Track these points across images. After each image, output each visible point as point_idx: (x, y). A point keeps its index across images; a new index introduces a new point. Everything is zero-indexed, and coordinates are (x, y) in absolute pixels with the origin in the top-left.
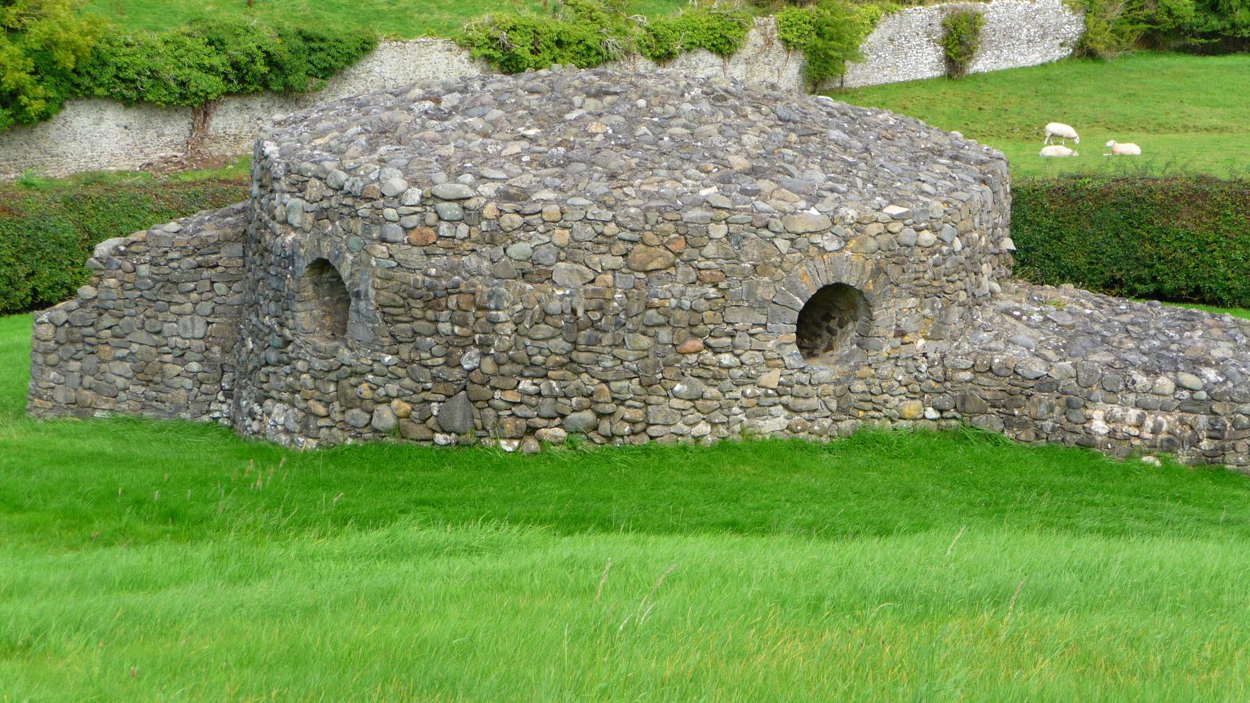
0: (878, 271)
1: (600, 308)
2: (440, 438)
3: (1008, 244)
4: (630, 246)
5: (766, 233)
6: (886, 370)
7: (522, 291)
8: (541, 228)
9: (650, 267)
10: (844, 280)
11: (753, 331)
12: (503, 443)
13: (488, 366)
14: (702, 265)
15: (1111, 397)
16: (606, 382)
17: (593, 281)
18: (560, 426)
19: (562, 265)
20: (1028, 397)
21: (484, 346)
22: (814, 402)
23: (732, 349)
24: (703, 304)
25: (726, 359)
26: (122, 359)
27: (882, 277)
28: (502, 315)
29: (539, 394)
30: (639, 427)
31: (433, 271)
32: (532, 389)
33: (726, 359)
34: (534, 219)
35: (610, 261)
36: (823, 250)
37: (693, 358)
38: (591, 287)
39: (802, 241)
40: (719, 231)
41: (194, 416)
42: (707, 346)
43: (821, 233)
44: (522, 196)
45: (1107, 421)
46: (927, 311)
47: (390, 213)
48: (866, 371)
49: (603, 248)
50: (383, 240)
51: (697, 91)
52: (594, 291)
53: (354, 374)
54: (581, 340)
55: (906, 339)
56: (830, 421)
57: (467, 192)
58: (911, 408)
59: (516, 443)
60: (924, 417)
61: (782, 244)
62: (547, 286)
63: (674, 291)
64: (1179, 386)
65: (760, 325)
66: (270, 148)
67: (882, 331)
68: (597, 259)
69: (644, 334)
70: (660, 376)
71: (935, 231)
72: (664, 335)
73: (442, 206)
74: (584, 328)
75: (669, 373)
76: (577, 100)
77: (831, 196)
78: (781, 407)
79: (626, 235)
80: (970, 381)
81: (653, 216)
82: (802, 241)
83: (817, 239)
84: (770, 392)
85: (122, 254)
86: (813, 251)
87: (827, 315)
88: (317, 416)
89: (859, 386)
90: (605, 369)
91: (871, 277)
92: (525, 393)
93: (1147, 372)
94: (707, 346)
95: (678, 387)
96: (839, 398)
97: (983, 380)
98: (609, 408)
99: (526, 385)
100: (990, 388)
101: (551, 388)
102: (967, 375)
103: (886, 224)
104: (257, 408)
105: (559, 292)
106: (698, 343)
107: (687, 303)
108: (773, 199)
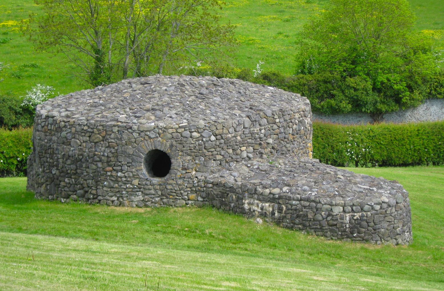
0: (172, 146)
4: (90, 134)
5: (130, 130)
6: (180, 182)
7: (63, 148)
8: (68, 127)
9: (95, 141)
11: (128, 165)
12: (62, 199)
13: (57, 173)
14: (109, 141)
15: (251, 196)
16: (86, 180)
17: (81, 146)
18: (75, 194)
19: (73, 139)
20: (228, 194)
21: (57, 166)
22: (153, 192)
23: (121, 171)
24: (110, 155)
25: (119, 174)
28: (60, 156)
29: (69, 183)
30: (95, 196)
32: (68, 181)
33: (119, 174)
36: (150, 138)
37: (109, 174)
38: (80, 147)
40: (116, 129)
43: (149, 131)
45: (249, 204)
46: (197, 161)
48: (171, 181)
49: (83, 134)
52: (81, 149)
54: (78, 165)
55: (188, 171)
56: (159, 198)
59: (65, 199)
60: (198, 200)
61: (135, 135)
62: (69, 147)
65: (130, 163)
67: (175, 167)
68: (81, 138)
69: (94, 164)
70: (99, 179)
71: (199, 132)
72: (100, 165)
78: (140, 193)
79: (89, 130)
80: (211, 188)
82: (142, 134)
83: (148, 133)
84: (135, 186)
86: (147, 138)
90: (85, 176)
91: (170, 148)
92: (66, 183)
96: (162, 190)
97: (215, 187)
98: (87, 189)
101: (73, 182)
102: (210, 185)
103: (176, 129)
105: (72, 149)
106: (111, 168)
107: (106, 154)
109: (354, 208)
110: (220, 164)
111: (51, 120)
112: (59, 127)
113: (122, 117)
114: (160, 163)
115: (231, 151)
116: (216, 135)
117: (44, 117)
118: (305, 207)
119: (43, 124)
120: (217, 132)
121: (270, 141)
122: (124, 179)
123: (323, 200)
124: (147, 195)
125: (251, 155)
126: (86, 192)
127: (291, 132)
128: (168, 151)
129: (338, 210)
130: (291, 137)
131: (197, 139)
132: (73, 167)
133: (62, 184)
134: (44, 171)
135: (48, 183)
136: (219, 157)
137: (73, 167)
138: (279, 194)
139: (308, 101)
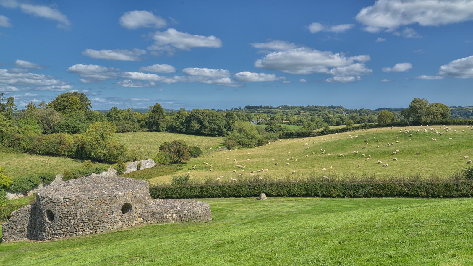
2: (70, 233)
3: (149, 194)
25: (112, 216)
26: (18, 229)
31: (66, 209)
34: (81, 200)
35: (93, 204)
39: (121, 198)
40: (109, 198)
41: (30, 236)
42: (109, 214)
44: (79, 196)
47: (59, 201)
50: (58, 206)
51: (103, 178)
53: (56, 226)
54: (90, 216)
57: (70, 197)
58: (139, 219)
64: (175, 210)
66: (39, 194)
73: (66, 199)
75: (104, 219)
76: (85, 182)
77: (124, 191)
81: (99, 197)
82: (121, 198)
83: (123, 197)
85: (16, 213)
87: (126, 208)
88: (50, 233)
93: (170, 209)
94: (109, 214)
95: (105, 221)
99: (82, 224)
100: (150, 214)
104: (40, 233)
108: (116, 192)
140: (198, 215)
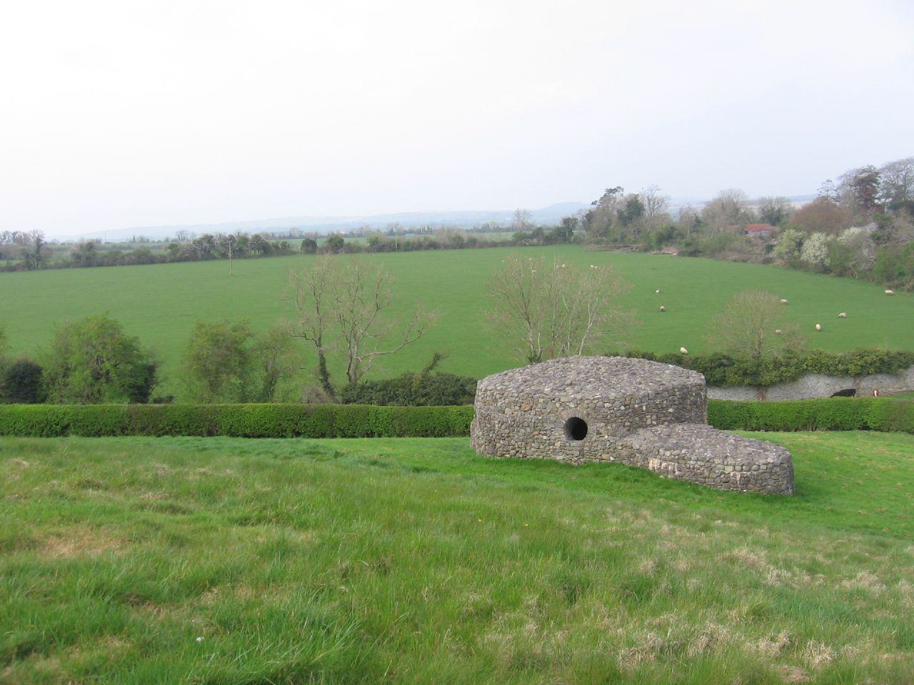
1: (514, 421)
10: (577, 416)
22: (571, 452)
23: (545, 434)
27: (590, 416)
33: (545, 437)
40: (541, 400)
58: (604, 456)
61: (558, 405)
63: (531, 416)
72: (528, 430)
74: (515, 425)
83: (568, 404)
89: (586, 448)
98: (518, 450)
100: (625, 452)
109: (744, 468)
110: (629, 430)
111: (489, 393)
112: (496, 398)
113: (547, 390)
114: (577, 429)
115: (637, 419)
116: (625, 406)
117: (483, 389)
118: (701, 466)
119: (483, 396)
120: (627, 403)
121: (671, 410)
122: (548, 442)
123: (717, 461)
124: (568, 455)
125: (654, 423)
126: (518, 452)
127: (689, 402)
128: (585, 419)
129: (729, 469)
130: (689, 408)
131: (609, 409)
132: (507, 431)
133: (498, 445)
134: (483, 434)
135: (487, 444)
136: (627, 424)
137: (507, 431)
138: (678, 455)
139: (703, 377)
140: (722, 476)
